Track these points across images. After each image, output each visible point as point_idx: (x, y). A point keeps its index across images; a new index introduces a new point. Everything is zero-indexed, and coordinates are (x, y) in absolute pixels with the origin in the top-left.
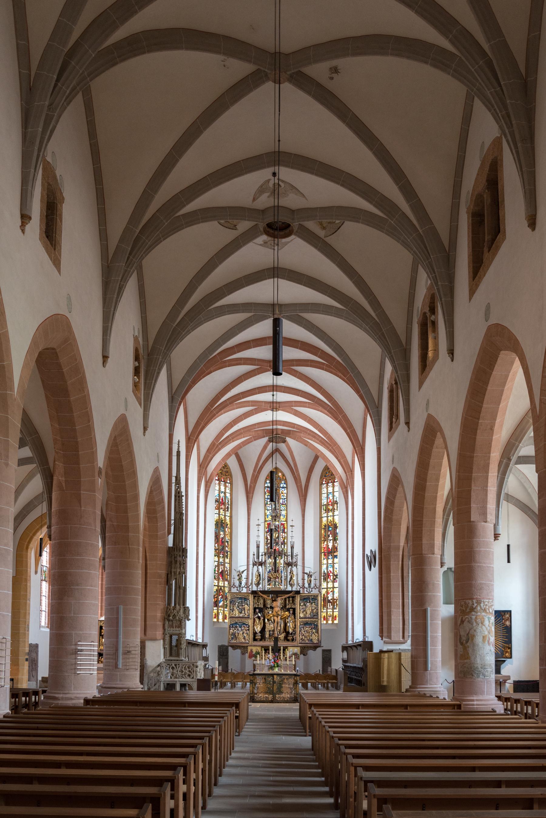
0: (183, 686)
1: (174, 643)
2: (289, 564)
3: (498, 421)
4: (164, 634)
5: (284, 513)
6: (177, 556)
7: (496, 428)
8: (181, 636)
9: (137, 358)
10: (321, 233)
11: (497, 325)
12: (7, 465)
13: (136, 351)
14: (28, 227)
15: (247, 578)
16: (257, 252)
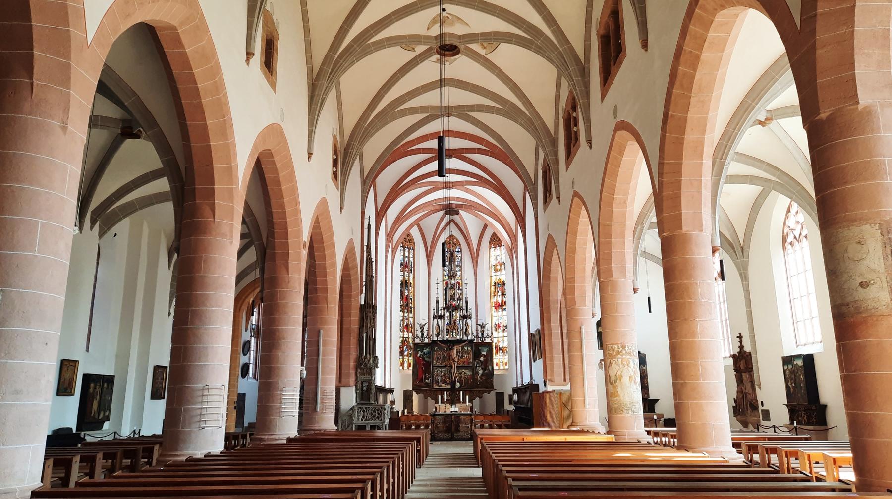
0: (373, 427)
1: (365, 389)
2: (464, 317)
3: (630, 196)
4: (356, 380)
5: (459, 273)
6: (368, 311)
7: (628, 202)
8: (371, 382)
9: (335, 152)
10: (482, 52)
11: (623, 122)
12: (232, 243)
13: (335, 146)
14: (251, 61)
15: (428, 330)
16: (429, 70)
